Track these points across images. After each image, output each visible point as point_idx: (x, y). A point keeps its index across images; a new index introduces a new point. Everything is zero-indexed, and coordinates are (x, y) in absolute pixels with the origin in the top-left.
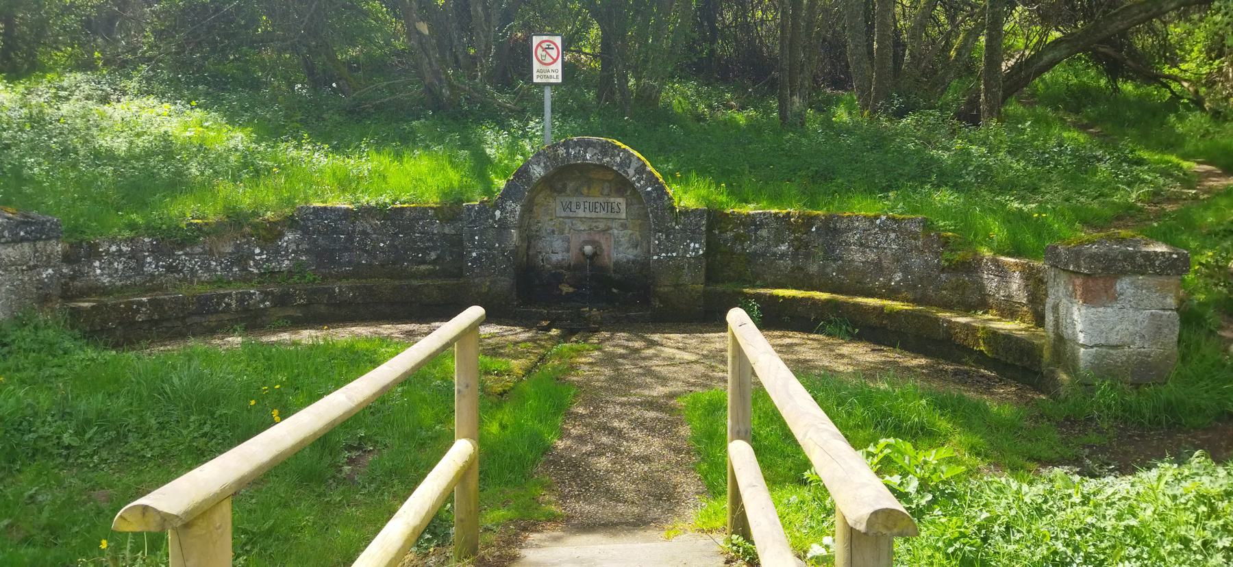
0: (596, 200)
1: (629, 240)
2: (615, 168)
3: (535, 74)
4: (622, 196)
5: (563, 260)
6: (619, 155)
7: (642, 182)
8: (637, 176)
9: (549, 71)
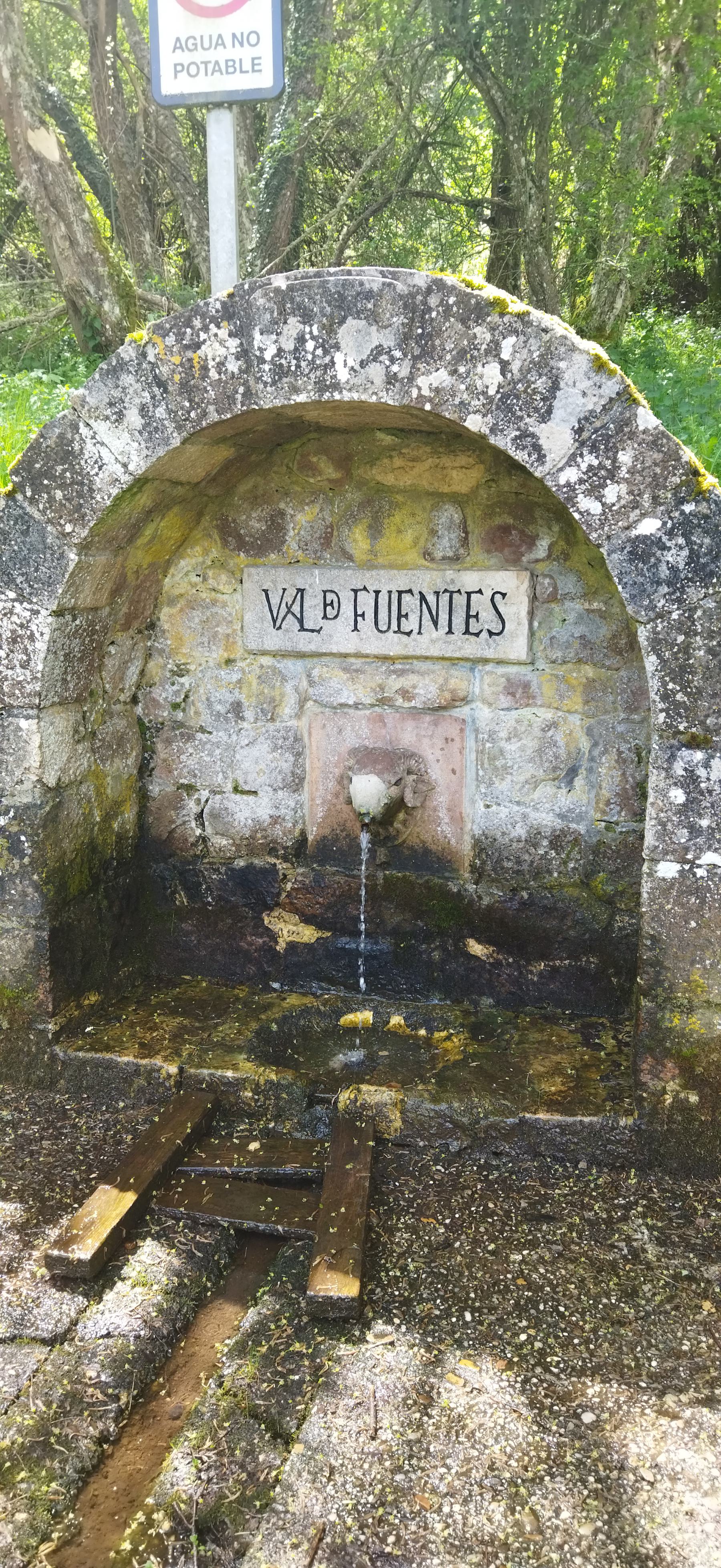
0: (401, 581)
1: (540, 751)
2: (475, 423)
3: (167, 59)
4: (514, 562)
5: (275, 820)
6: (494, 349)
7: (611, 493)
8: (590, 459)
9: (220, 41)
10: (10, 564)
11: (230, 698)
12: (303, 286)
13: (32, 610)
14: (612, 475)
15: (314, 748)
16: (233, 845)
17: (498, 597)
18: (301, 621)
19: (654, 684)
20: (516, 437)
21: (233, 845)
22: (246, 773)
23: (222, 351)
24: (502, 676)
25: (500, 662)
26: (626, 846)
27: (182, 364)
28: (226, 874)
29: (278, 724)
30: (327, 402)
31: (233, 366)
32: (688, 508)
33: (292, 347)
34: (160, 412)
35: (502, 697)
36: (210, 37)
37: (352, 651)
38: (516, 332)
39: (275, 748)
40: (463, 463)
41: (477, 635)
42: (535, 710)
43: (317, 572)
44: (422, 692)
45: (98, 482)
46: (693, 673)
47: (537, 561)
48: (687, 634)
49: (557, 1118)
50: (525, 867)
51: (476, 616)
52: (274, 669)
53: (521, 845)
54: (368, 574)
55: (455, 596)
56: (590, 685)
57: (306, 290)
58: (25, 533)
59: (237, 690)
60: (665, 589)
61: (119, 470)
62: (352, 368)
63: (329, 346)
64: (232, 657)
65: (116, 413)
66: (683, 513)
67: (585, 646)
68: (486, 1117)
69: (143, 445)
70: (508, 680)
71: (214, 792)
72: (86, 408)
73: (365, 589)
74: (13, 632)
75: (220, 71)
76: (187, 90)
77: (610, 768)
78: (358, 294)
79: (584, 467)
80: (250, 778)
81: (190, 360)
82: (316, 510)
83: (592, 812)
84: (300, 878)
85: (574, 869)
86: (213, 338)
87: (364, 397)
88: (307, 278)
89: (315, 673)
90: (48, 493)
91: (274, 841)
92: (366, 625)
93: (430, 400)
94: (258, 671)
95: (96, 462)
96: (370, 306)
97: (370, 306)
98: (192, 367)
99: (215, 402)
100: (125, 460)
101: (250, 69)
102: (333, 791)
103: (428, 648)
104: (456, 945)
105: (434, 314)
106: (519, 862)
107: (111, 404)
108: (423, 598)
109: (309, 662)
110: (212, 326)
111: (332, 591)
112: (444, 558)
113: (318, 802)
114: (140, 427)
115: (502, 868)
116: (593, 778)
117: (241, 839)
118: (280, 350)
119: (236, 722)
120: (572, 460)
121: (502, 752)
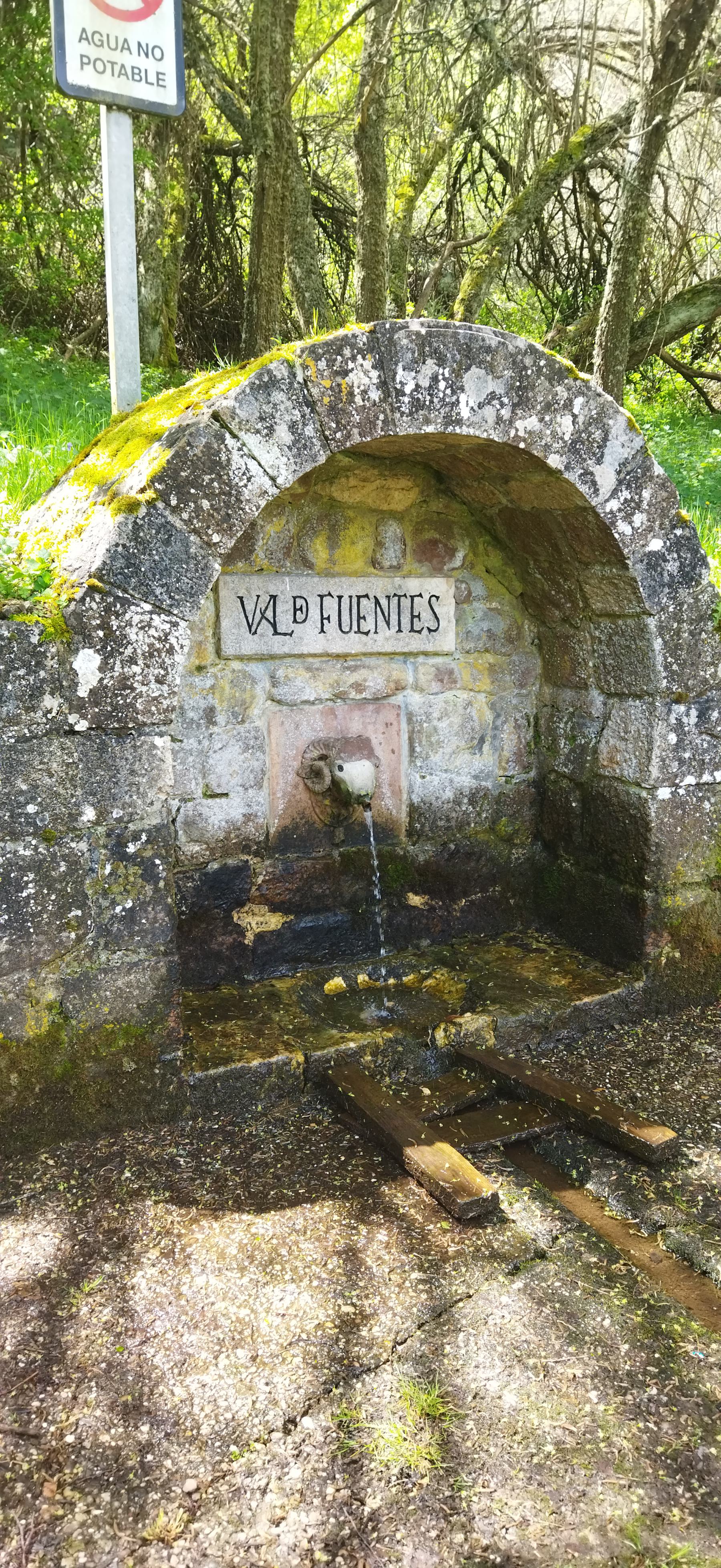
0: (359, 587)
1: (462, 726)
2: (554, 461)
4: (437, 571)
5: (248, 817)
6: (568, 405)
7: (639, 519)
8: (625, 494)
9: (125, 46)
10: (150, 575)
11: (203, 704)
12: (439, 335)
13: (171, 622)
14: (638, 506)
15: (274, 745)
16: (206, 850)
17: (434, 599)
18: (274, 625)
19: (660, 659)
20: (582, 475)
21: (206, 850)
22: (220, 777)
23: (366, 381)
24: (433, 666)
25: (436, 654)
26: (519, 793)
27: (331, 388)
28: (200, 879)
29: (246, 725)
30: (450, 434)
31: (375, 395)
32: (679, 532)
33: (427, 385)
34: (309, 431)
35: (433, 683)
36: (117, 38)
37: (320, 651)
38: (583, 394)
39: (247, 748)
40: (403, 486)
41: (419, 632)
42: (454, 692)
43: (287, 579)
44: (371, 684)
45: (246, 494)
46: (682, 650)
47: (454, 569)
48: (679, 623)
49: (597, 998)
50: (453, 823)
51: (418, 616)
52: (244, 673)
53: (450, 805)
54: (332, 581)
55: (402, 599)
56: (492, 669)
57: (441, 338)
58: (167, 542)
59: (211, 696)
60: (667, 590)
61: (268, 483)
62: (472, 408)
63: (456, 388)
64: (203, 664)
65: (267, 428)
66: (675, 535)
67: (489, 637)
68: (553, 1013)
69: (292, 461)
70: (438, 669)
71: (184, 800)
72: (237, 420)
73: (330, 594)
74: (151, 646)
75: (126, 74)
76: (94, 85)
77: (510, 734)
78: (481, 347)
79: (622, 499)
80: (224, 781)
81: (339, 385)
82: (283, 522)
83: (497, 771)
84: (270, 870)
85: (486, 818)
86: (359, 368)
87: (477, 433)
88: (437, 327)
89: (280, 673)
90: (195, 502)
91: (248, 839)
92: (331, 627)
93: (524, 440)
94: (230, 676)
95: (244, 474)
96: (489, 359)
97: (489, 359)
98: (341, 391)
99: (359, 425)
100: (275, 473)
101: (155, 82)
102: (293, 783)
103: (383, 645)
104: (400, 902)
105: (529, 372)
106: (448, 820)
107: (262, 419)
108: (377, 602)
109: (271, 664)
110: (359, 357)
111: (301, 597)
112: (391, 567)
113: (279, 795)
114: (289, 443)
115: (437, 827)
116: (497, 743)
117: (217, 841)
118: (418, 386)
119: (207, 728)
120: (614, 493)
121: (435, 729)
